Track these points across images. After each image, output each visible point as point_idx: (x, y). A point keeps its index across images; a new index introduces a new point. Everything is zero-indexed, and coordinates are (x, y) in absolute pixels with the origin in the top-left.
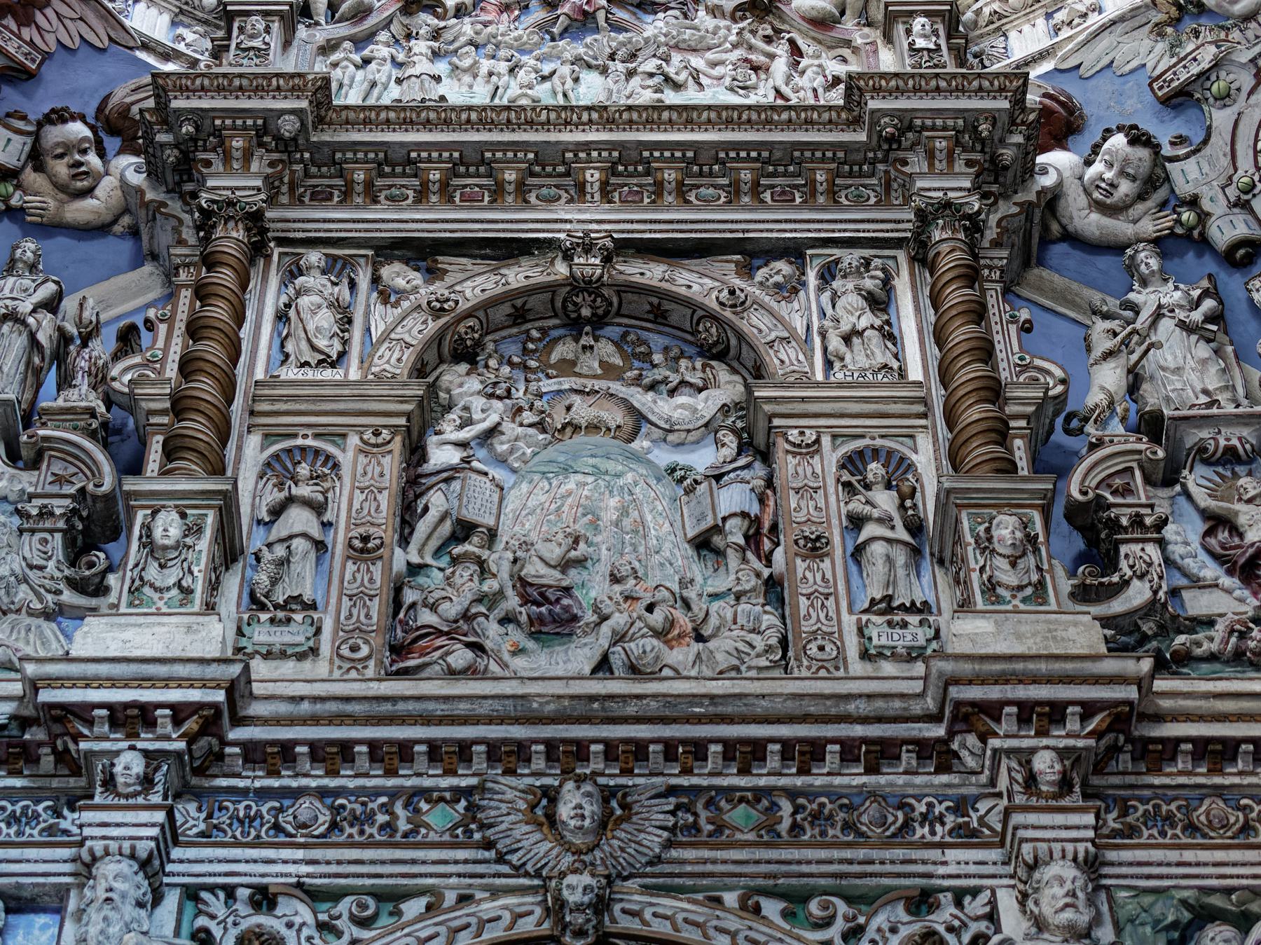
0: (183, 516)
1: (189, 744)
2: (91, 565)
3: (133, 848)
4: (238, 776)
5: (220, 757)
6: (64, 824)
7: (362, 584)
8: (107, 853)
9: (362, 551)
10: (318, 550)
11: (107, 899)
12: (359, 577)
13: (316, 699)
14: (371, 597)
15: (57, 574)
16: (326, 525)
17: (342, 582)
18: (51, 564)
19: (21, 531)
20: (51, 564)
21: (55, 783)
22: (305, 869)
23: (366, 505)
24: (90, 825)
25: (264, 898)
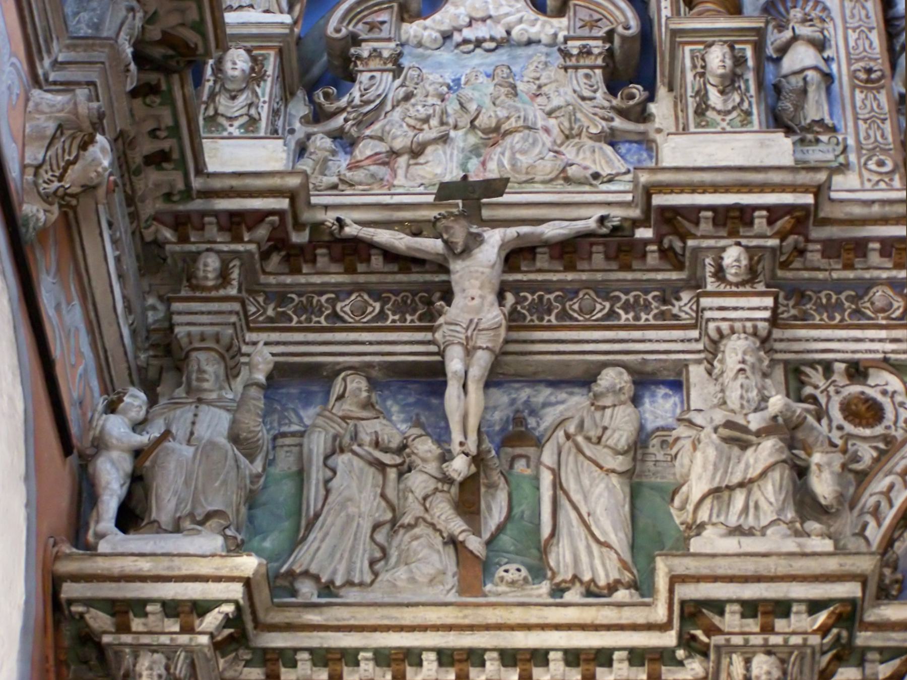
0: (732, 47)
1: (782, 240)
2: (632, 97)
3: (755, 327)
4: (818, 269)
5: (801, 252)
6: (675, 311)
7: (872, 110)
8: (733, 331)
9: (868, 81)
10: (826, 82)
11: (741, 370)
12: (868, 103)
13: (883, 202)
14: (883, 121)
15: (606, 104)
16: (827, 60)
17: (854, 107)
18: (599, 95)
19: (566, 69)
20: (599, 95)
21: (660, 276)
22: (889, 347)
23: (860, 42)
24: (711, 309)
25: (857, 371)
